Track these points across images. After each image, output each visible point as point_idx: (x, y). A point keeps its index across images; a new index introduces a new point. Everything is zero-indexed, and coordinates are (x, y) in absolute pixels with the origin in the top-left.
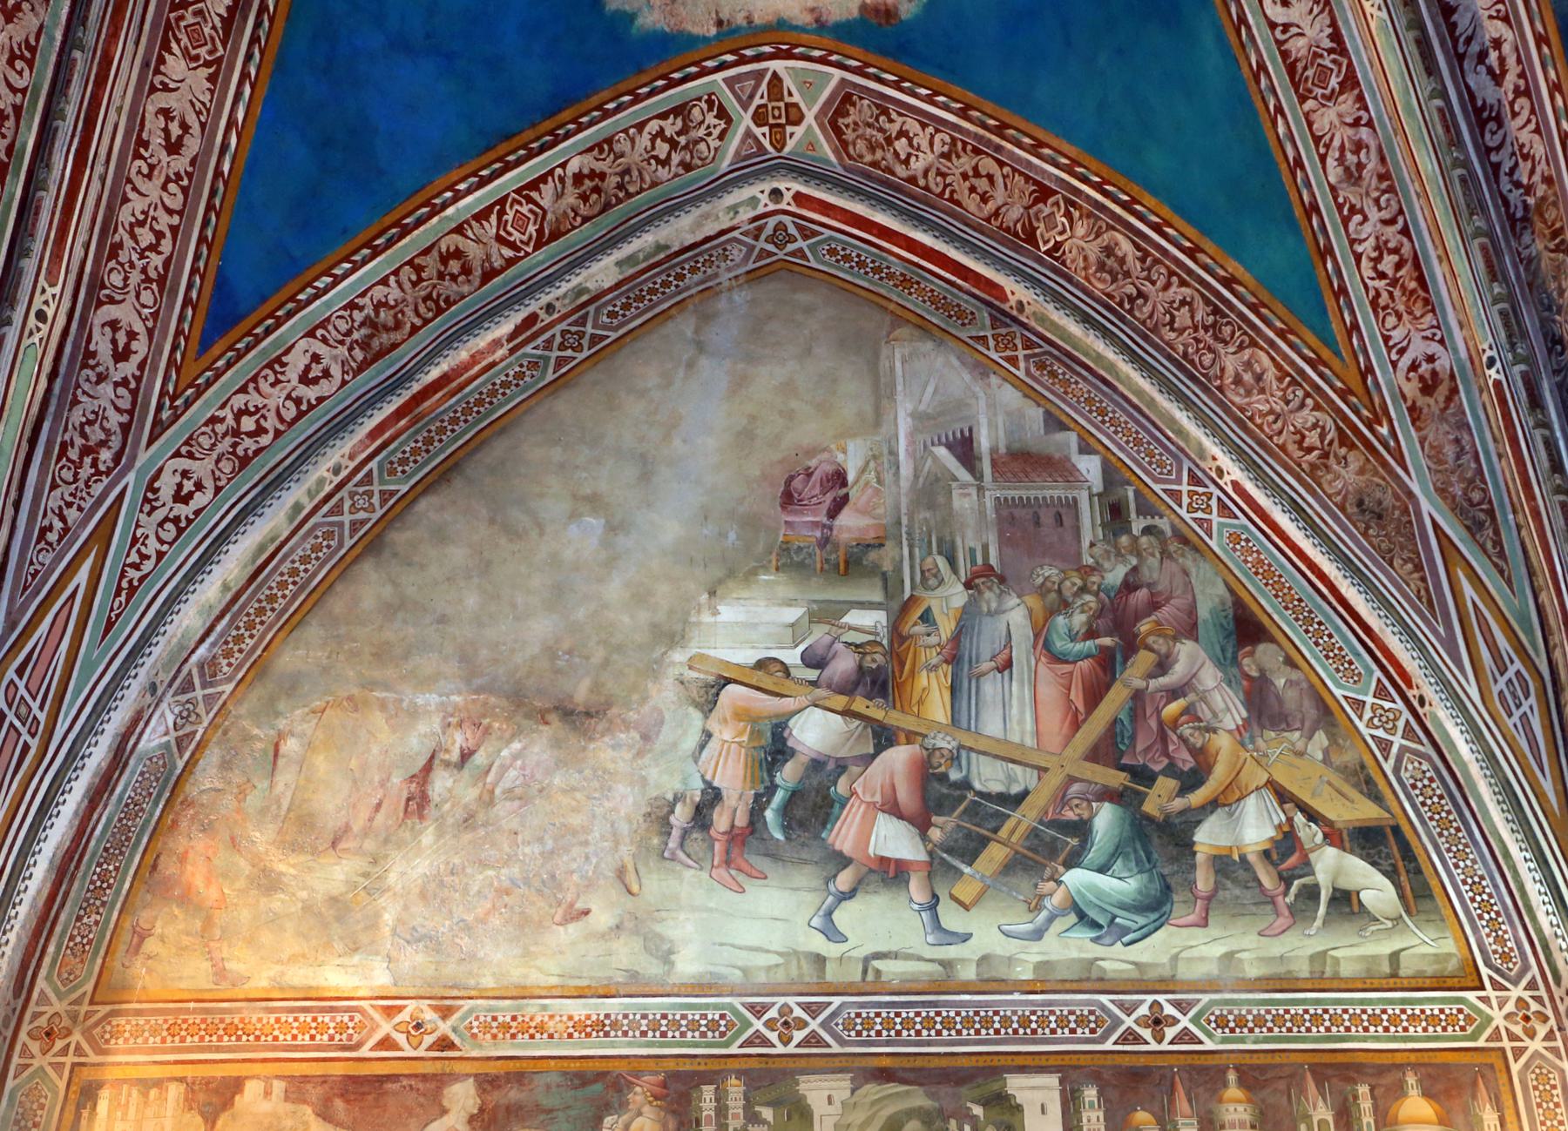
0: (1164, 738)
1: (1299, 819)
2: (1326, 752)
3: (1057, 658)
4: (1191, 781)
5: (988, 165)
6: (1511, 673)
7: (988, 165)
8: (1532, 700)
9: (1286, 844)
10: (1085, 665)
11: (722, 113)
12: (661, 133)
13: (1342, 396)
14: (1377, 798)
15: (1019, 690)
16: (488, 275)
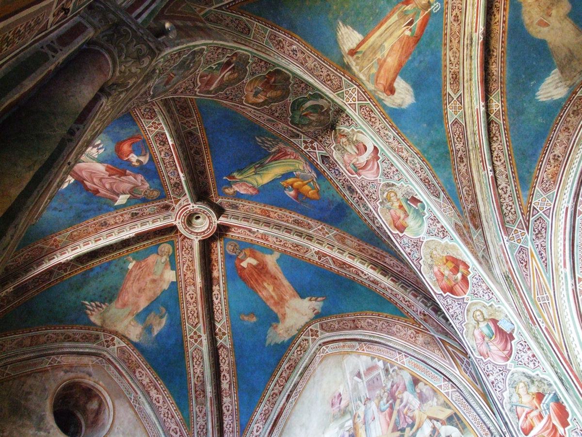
0: (405, 418)
1: (435, 422)
2: (437, 402)
3: (382, 411)
4: (412, 426)
5: (344, 322)
6: (465, 362)
7: (344, 322)
8: (471, 366)
9: (434, 429)
10: (388, 410)
11: (306, 340)
12: (298, 351)
13: (412, 325)
14: (449, 408)
15: (377, 422)
16: (280, 393)
